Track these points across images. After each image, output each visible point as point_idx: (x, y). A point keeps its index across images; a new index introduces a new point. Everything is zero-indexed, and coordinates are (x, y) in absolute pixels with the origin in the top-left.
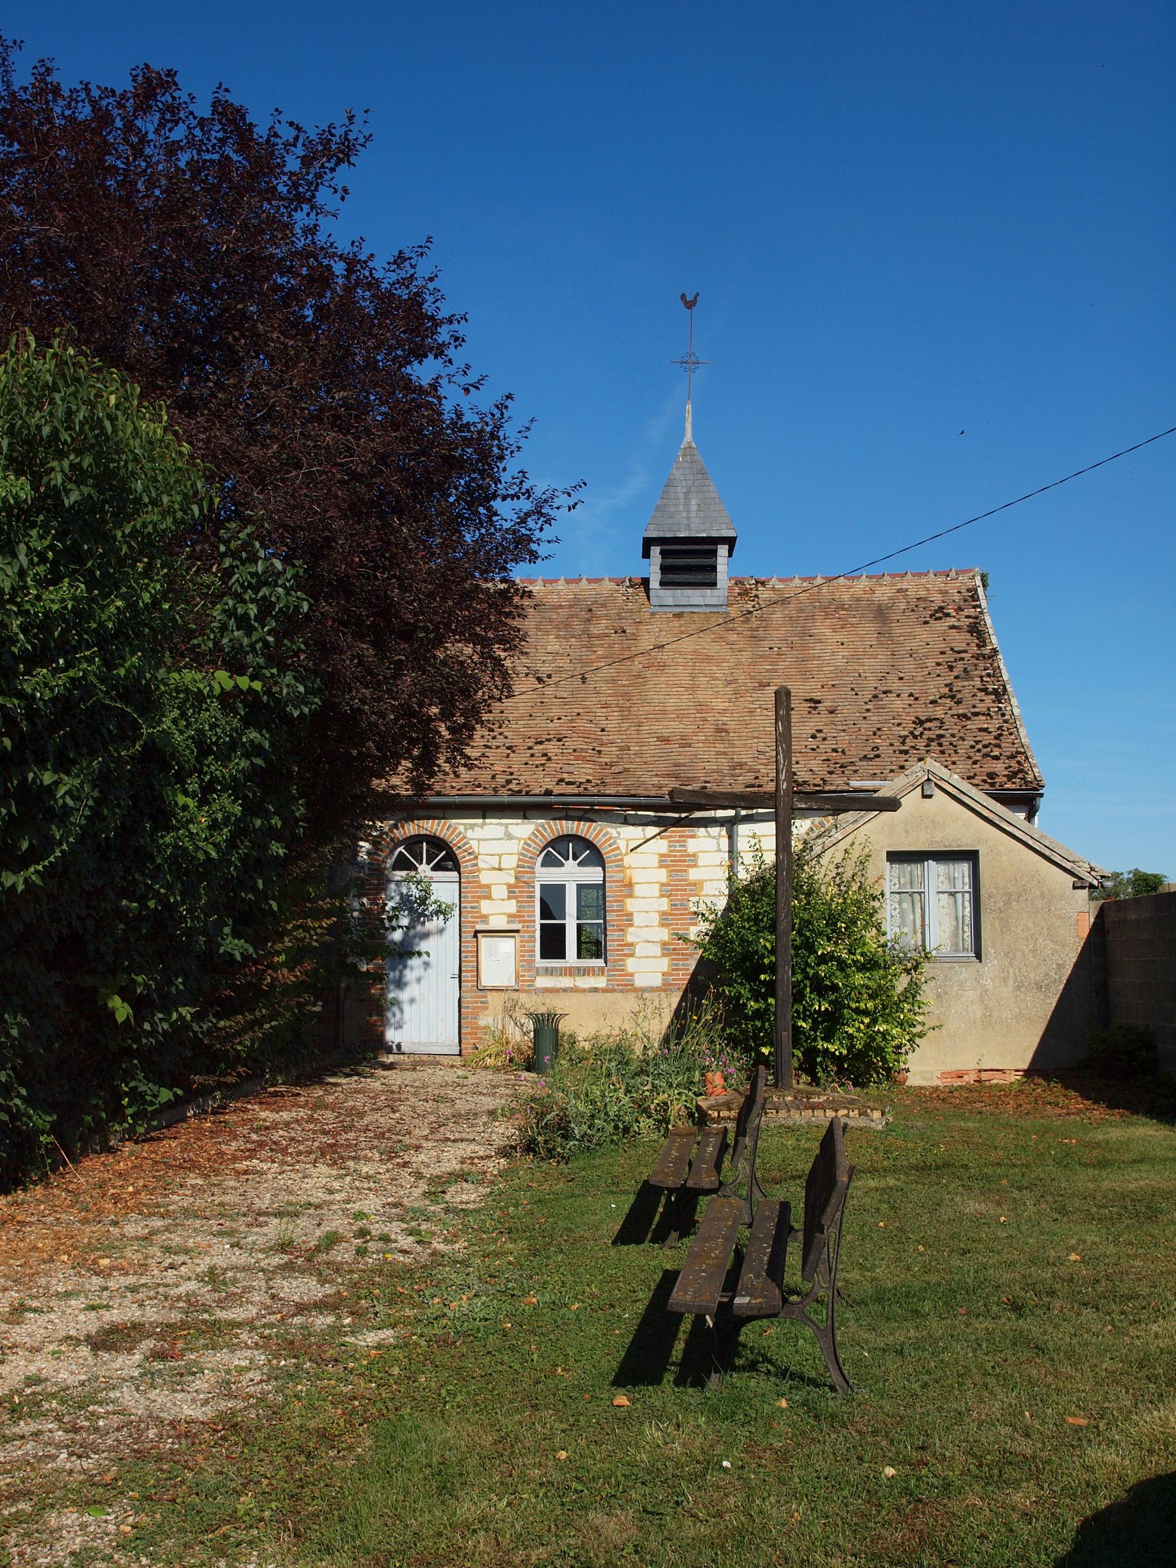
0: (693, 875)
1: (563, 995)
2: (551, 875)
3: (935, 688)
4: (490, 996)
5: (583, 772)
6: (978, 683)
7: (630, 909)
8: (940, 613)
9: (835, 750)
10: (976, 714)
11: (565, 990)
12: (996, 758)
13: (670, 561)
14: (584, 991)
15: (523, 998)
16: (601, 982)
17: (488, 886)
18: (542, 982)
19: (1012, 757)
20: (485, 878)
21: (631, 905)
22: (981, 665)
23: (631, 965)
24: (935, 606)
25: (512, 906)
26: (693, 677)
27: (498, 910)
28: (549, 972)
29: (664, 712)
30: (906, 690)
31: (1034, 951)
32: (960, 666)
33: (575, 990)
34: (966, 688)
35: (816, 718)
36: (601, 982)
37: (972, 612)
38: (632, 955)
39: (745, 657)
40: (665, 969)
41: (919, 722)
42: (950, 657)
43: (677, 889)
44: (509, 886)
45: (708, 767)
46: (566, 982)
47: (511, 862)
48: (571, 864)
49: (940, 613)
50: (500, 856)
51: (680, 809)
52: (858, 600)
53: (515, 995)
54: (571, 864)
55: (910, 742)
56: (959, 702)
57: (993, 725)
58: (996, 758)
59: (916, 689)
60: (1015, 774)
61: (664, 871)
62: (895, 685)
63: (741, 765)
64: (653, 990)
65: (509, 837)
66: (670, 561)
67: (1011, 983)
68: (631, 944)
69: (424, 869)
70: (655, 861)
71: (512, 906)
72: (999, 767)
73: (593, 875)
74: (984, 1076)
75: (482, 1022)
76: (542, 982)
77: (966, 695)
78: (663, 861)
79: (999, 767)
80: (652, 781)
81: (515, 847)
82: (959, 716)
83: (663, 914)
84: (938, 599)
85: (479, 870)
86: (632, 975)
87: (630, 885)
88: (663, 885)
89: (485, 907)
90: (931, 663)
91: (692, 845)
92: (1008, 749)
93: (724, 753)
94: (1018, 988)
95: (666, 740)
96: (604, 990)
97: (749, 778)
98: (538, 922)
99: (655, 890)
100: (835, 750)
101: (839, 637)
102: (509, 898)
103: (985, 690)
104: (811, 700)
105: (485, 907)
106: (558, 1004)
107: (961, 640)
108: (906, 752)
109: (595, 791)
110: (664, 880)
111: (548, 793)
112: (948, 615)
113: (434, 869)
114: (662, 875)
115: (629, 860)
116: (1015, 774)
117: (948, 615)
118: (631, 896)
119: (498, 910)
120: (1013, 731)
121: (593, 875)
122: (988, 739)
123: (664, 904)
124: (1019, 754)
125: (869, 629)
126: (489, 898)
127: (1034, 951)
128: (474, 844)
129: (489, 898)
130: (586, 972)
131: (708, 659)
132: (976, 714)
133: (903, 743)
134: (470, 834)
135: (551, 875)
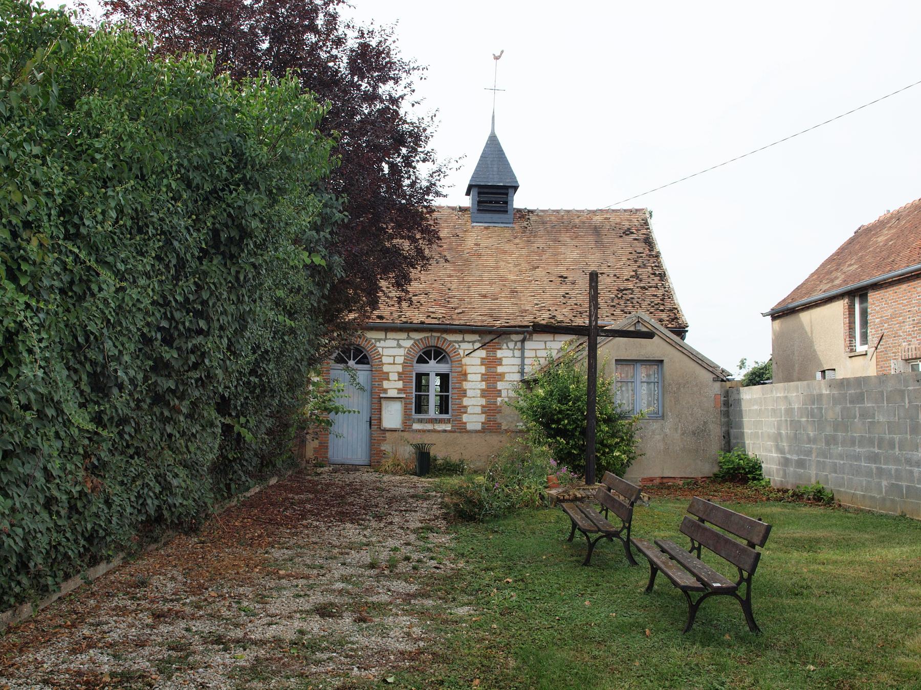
0: (500, 369)
1: (427, 434)
2: (423, 368)
3: (627, 273)
4: (388, 434)
5: (440, 311)
6: (650, 269)
7: (465, 387)
8: (628, 232)
9: (576, 304)
10: (651, 287)
11: (429, 431)
12: (662, 311)
13: (485, 198)
14: (439, 431)
15: (406, 434)
16: (448, 427)
17: (388, 373)
18: (416, 426)
19: (670, 310)
20: (386, 369)
21: (466, 385)
22: (652, 260)
23: (465, 418)
24: (625, 228)
25: (400, 385)
26: (497, 262)
27: (393, 386)
28: (420, 421)
29: (482, 281)
30: (612, 273)
31: (692, 414)
32: (640, 260)
33: (434, 431)
34: (644, 273)
35: (564, 287)
36: (448, 427)
37: (644, 231)
38: (465, 413)
39: (524, 252)
40: (483, 420)
41: (620, 290)
42: (635, 256)
43: (491, 378)
44: (399, 373)
45: (508, 312)
46: (429, 427)
47: (400, 360)
48: (432, 362)
49: (628, 232)
50: (394, 357)
51: (492, 335)
52: (584, 223)
53: (403, 434)
54: (432, 362)
55: (616, 301)
56: (641, 281)
57: (660, 293)
58: (662, 311)
59: (617, 272)
60: (673, 320)
61: (483, 367)
62: (606, 270)
63: (526, 311)
64: (477, 432)
65: (399, 346)
66: (485, 198)
67: (679, 431)
68: (465, 407)
69: (351, 363)
70: (479, 362)
71: (400, 385)
72: (664, 316)
73: (443, 368)
74: (665, 481)
75: (383, 448)
76: (416, 426)
77: (644, 277)
78: (483, 362)
79: (664, 316)
80: (476, 318)
81: (402, 352)
82: (642, 288)
83: (482, 390)
84: (626, 224)
85: (383, 364)
86: (465, 423)
87: (465, 374)
88: (483, 375)
89: (386, 384)
90: (624, 259)
91: (499, 354)
92: (668, 306)
93: (516, 304)
94: (683, 434)
95: (485, 296)
96: (450, 431)
97: (531, 318)
98: (414, 393)
99: (479, 377)
100: (576, 304)
101: (574, 243)
102: (399, 380)
103: (654, 274)
104: (561, 277)
105: (386, 384)
106: (426, 439)
107: (640, 247)
108: (614, 306)
109: (448, 322)
110: (484, 372)
111: (422, 323)
112: (632, 233)
113: (356, 363)
114: (483, 369)
115: (466, 361)
116: (673, 320)
117: (632, 233)
118: (466, 380)
119: (393, 386)
120: (670, 297)
121: (443, 368)
122: (657, 300)
123: (483, 385)
124: (674, 310)
125: (591, 239)
126: (388, 379)
127: (692, 414)
128: (380, 350)
129: (388, 379)
130: (441, 421)
131: (505, 252)
132: (651, 287)
133: (613, 301)
134: (378, 344)
135: (423, 368)
